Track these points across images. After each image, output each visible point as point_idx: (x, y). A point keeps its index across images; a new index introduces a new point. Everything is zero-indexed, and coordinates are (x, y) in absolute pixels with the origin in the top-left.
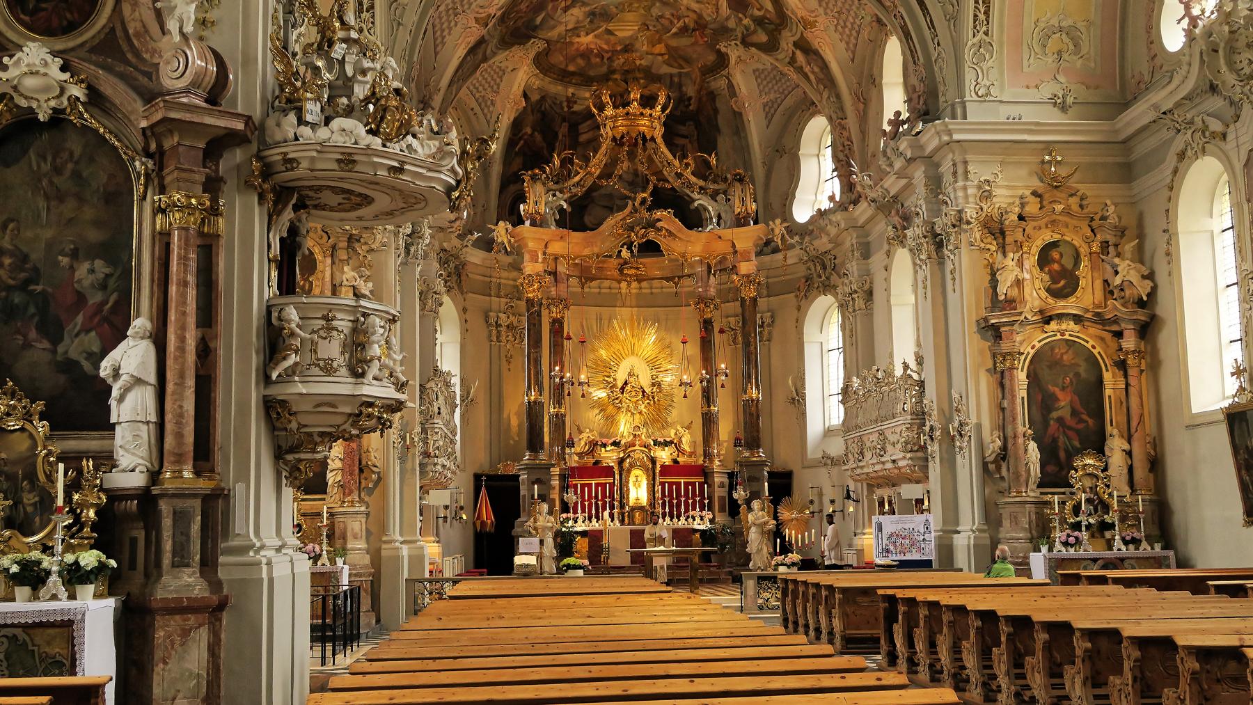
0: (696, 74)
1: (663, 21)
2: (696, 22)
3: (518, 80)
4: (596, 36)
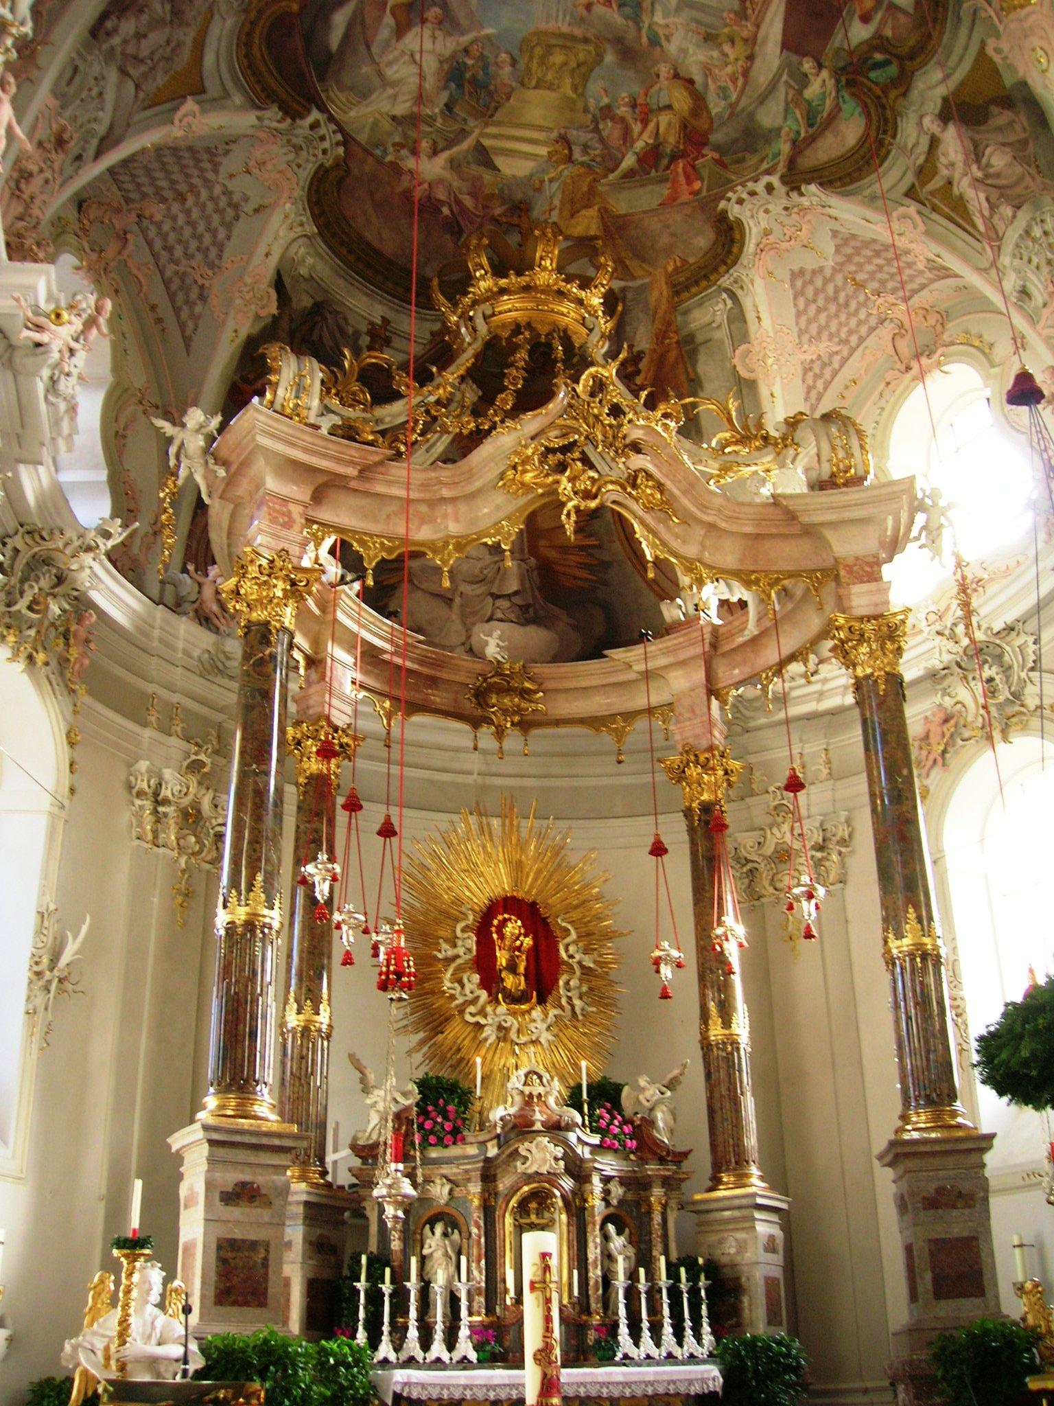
0: (659, 293)
1: (609, 129)
2: (684, 126)
3: (267, 238)
4: (454, 165)
